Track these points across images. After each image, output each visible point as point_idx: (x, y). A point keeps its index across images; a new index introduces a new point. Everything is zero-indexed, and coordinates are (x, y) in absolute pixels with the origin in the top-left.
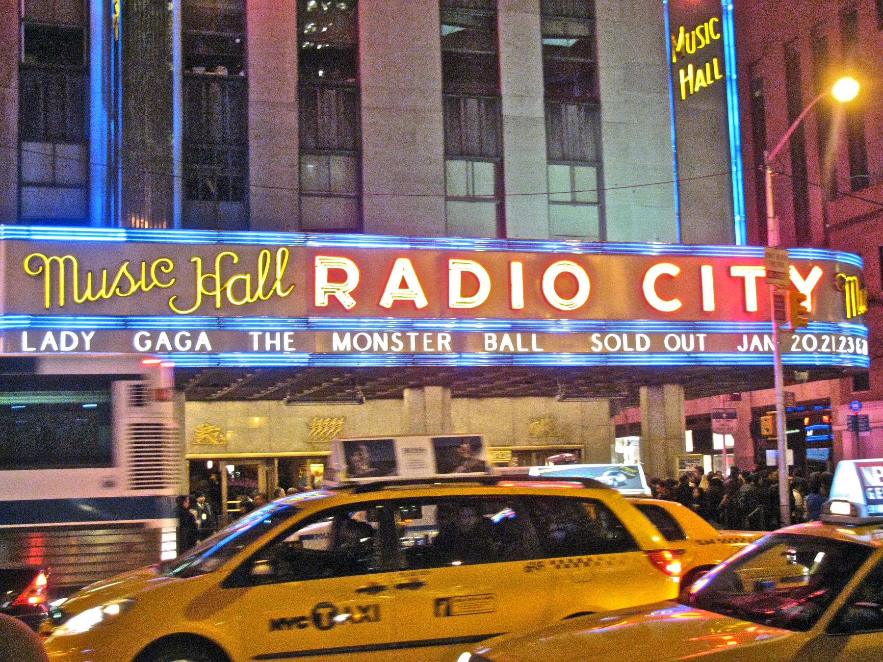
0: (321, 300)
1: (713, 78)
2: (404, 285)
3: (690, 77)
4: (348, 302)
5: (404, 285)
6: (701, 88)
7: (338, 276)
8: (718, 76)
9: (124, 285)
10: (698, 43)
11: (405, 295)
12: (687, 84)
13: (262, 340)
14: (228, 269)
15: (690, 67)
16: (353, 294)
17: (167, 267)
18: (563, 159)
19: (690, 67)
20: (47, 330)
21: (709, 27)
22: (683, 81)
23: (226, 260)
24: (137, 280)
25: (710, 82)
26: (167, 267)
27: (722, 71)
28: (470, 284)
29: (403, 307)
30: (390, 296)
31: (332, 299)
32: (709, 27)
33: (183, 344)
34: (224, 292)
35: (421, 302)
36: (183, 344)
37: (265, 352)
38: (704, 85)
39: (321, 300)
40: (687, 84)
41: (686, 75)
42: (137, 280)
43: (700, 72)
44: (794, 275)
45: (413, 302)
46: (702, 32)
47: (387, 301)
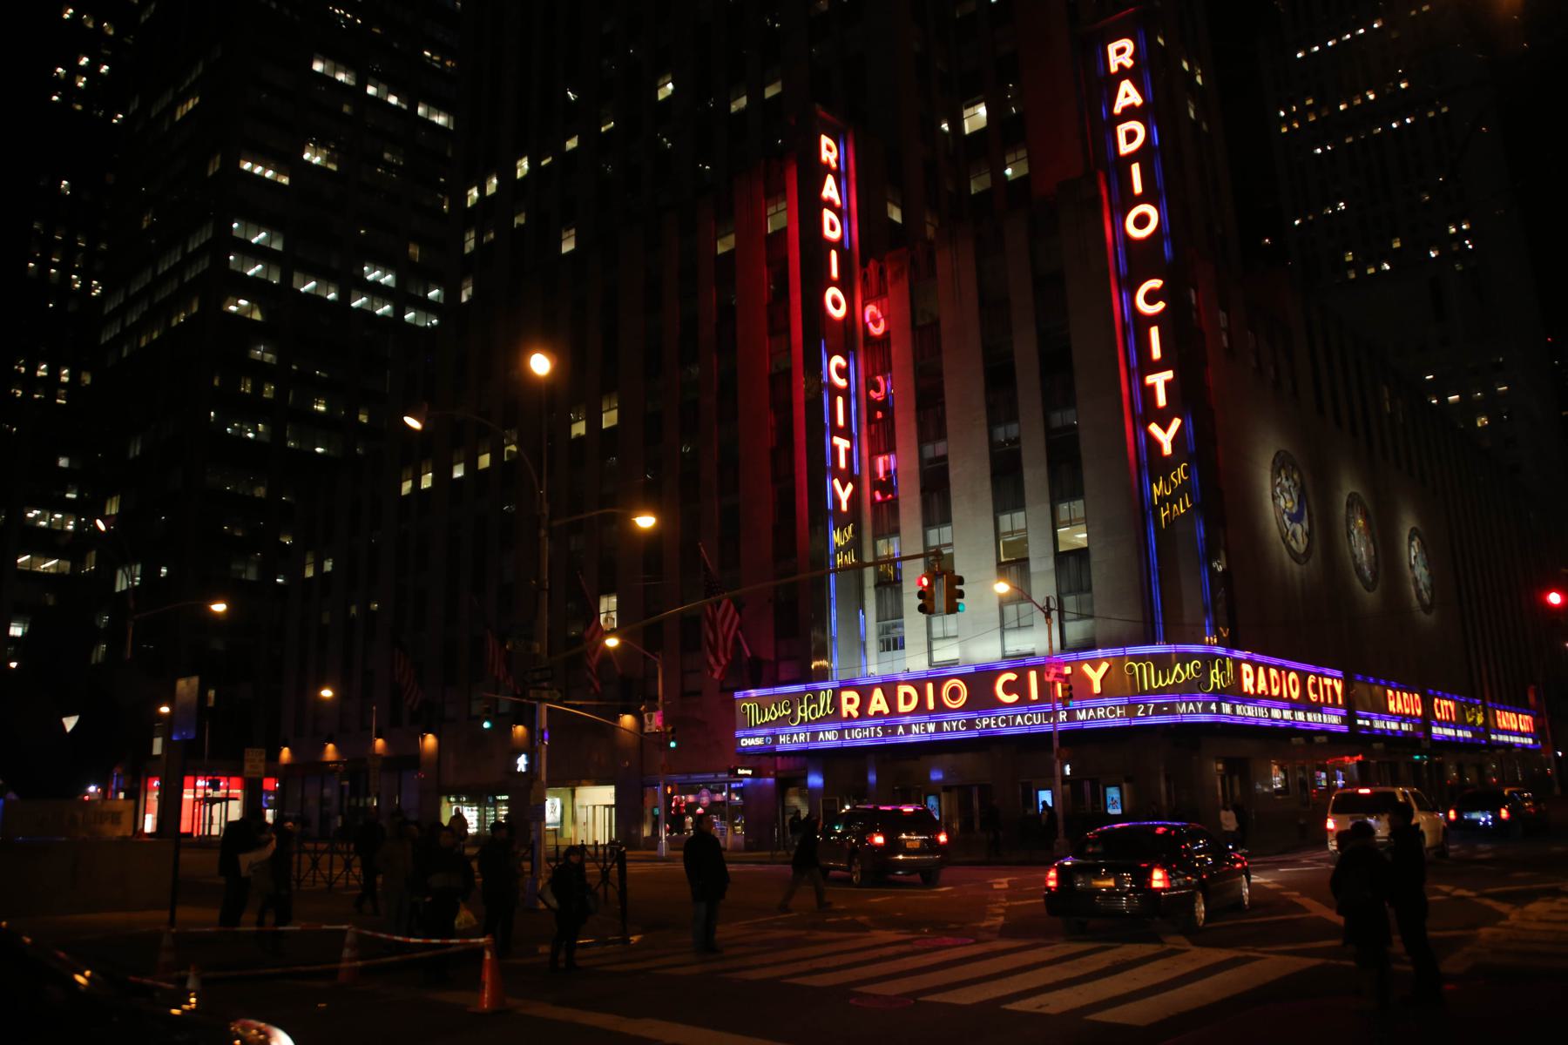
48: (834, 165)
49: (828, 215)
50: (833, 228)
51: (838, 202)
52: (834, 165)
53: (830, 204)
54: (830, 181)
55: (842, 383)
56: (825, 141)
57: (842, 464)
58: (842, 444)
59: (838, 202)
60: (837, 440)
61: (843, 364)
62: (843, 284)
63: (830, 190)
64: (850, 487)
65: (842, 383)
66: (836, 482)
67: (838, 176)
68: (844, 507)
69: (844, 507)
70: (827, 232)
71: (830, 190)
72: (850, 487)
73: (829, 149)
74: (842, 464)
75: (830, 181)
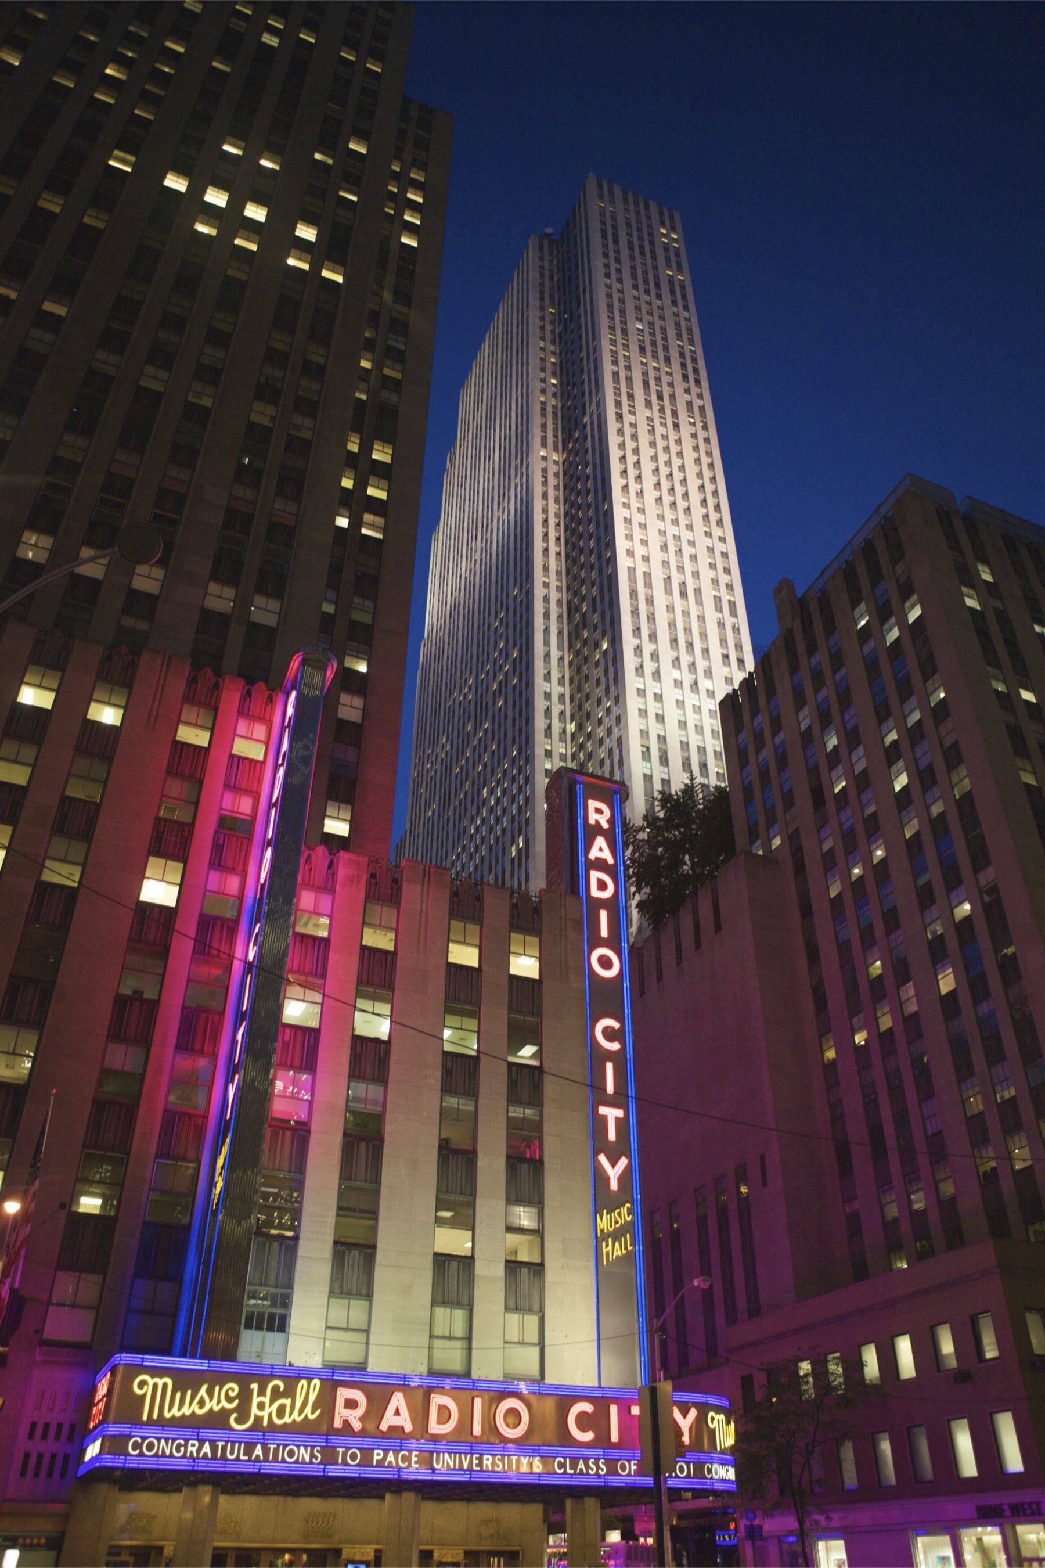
0: (338, 1424)
1: (626, 1248)
2: (397, 1413)
3: (610, 1248)
4: (357, 1426)
5: (397, 1413)
6: (617, 1257)
7: (351, 1404)
8: (630, 1248)
9: (202, 1404)
10: (616, 1222)
11: (397, 1421)
12: (607, 1254)
13: (276, 1451)
14: (276, 1394)
15: (610, 1240)
16: (360, 1419)
17: (233, 1390)
18: (517, 1309)
19: (610, 1240)
20: (257, 1443)
21: (624, 1211)
22: (605, 1250)
23: (276, 1388)
24: (211, 1399)
25: (624, 1252)
26: (233, 1390)
27: (633, 1244)
28: (444, 1414)
29: (396, 1431)
30: (389, 1420)
31: (346, 1423)
32: (624, 1211)
33: (178, 1451)
34: (270, 1415)
35: (408, 1428)
36: (178, 1451)
37: (277, 1462)
38: (619, 1253)
39: (338, 1424)
40: (607, 1254)
41: (607, 1246)
42: (211, 1399)
43: (617, 1244)
44: (677, 1414)
45: (403, 1428)
46: (619, 1214)
47: (384, 1427)
48: (605, 825)
49: (595, 875)
50: (602, 886)
51: (611, 861)
52: (605, 825)
53: (600, 865)
54: (600, 841)
55: (615, 1046)
56: (593, 804)
57: (612, 1136)
58: (612, 1114)
59: (611, 861)
60: (603, 1110)
61: (616, 1025)
62: (612, 942)
63: (600, 850)
64: (623, 1162)
65: (615, 1046)
66: (602, 1158)
67: (609, 836)
68: (614, 1185)
69: (614, 1185)
70: (595, 892)
71: (600, 850)
72: (623, 1162)
73: (599, 811)
74: (612, 1136)
75: (600, 841)
